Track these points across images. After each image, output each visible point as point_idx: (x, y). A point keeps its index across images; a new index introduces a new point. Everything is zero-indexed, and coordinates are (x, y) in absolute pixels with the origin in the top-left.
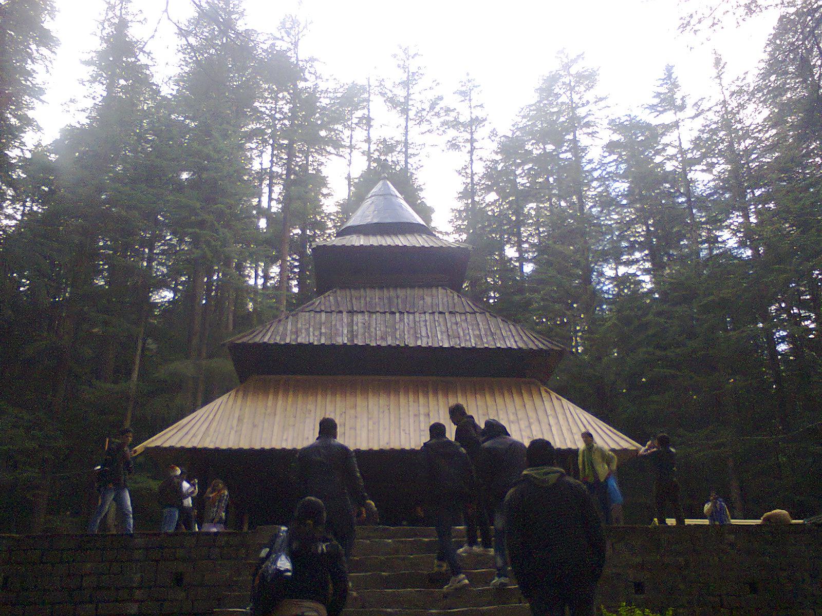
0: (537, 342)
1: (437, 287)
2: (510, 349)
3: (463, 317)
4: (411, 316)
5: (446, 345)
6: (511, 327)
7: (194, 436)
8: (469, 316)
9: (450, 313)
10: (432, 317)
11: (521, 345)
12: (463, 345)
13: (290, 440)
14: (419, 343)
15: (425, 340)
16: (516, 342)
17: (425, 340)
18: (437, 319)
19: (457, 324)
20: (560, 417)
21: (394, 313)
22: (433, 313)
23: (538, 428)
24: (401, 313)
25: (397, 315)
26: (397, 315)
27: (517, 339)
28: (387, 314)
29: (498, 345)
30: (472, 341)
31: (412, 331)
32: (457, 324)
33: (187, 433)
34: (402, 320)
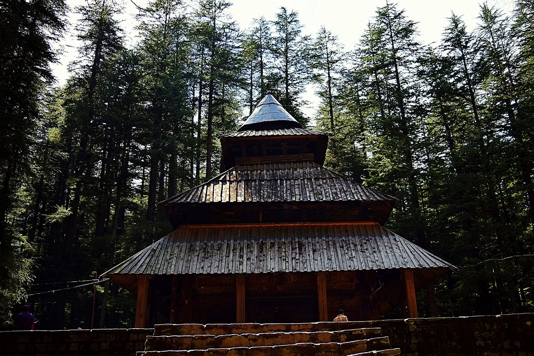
0: (376, 196)
1: (306, 162)
2: (358, 201)
5: (313, 200)
11: (364, 198)
12: (324, 199)
13: (205, 269)
14: (294, 199)
15: (298, 197)
16: (361, 196)
17: (298, 197)
18: (306, 182)
19: (320, 185)
20: (394, 247)
23: (379, 255)
27: (362, 194)
29: (349, 199)
30: (331, 196)
31: (289, 192)
32: (320, 185)
33: (136, 265)
34: (282, 184)
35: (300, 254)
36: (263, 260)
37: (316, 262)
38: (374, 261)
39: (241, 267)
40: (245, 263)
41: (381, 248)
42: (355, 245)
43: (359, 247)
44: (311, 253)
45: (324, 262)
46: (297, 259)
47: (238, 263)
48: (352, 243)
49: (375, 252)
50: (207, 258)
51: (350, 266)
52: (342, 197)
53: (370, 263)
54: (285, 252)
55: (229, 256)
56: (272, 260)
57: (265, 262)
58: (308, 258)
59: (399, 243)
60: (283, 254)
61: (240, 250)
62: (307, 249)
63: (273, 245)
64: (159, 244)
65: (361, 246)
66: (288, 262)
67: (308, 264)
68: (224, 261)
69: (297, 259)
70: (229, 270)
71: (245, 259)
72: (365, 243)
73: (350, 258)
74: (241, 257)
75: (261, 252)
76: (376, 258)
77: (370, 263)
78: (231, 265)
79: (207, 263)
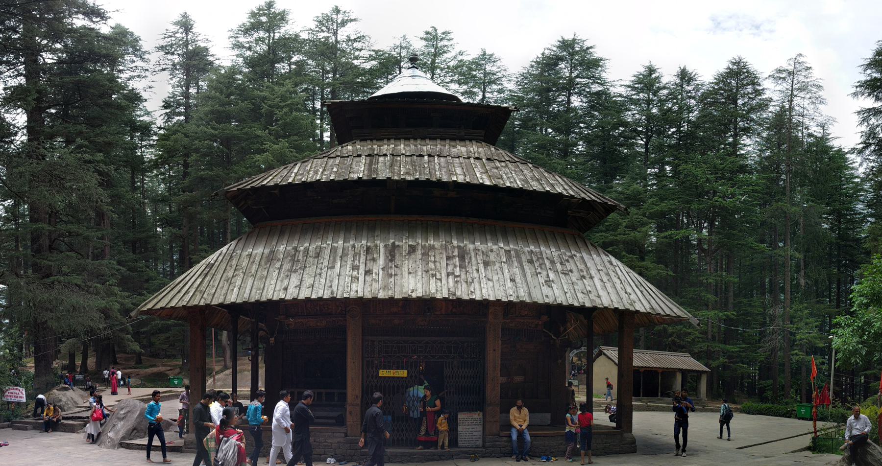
3: (503, 164)
4: (442, 159)
6: (557, 177)
8: (510, 165)
9: (488, 159)
10: (467, 161)
16: (566, 190)
20: (612, 274)
21: (422, 156)
22: (469, 158)
24: (430, 156)
25: (426, 157)
26: (426, 157)
27: (566, 187)
35: (461, 267)
36: (395, 275)
37: (490, 283)
38: (585, 291)
39: (354, 286)
41: (593, 272)
44: (481, 266)
46: (457, 276)
47: (348, 280)
49: (584, 277)
50: (296, 271)
52: (535, 186)
53: (580, 295)
54: (435, 262)
55: (333, 267)
56: (410, 276)
57: (398, 278)
58: (476, 275)
59: (617, 268)
60: (431, 265)
61: (355, 256)
62: (473, 259)
63: (412, 250)
66: (440, 280)
68: (324, 275)
69: (457, 276)
70: (332, 292)
71: (362, 271)
73: (546, 281)
74: (355, 268)
75: (391, 261)
76: (589, 288)
77: (580, 295)
79: (295, 280)
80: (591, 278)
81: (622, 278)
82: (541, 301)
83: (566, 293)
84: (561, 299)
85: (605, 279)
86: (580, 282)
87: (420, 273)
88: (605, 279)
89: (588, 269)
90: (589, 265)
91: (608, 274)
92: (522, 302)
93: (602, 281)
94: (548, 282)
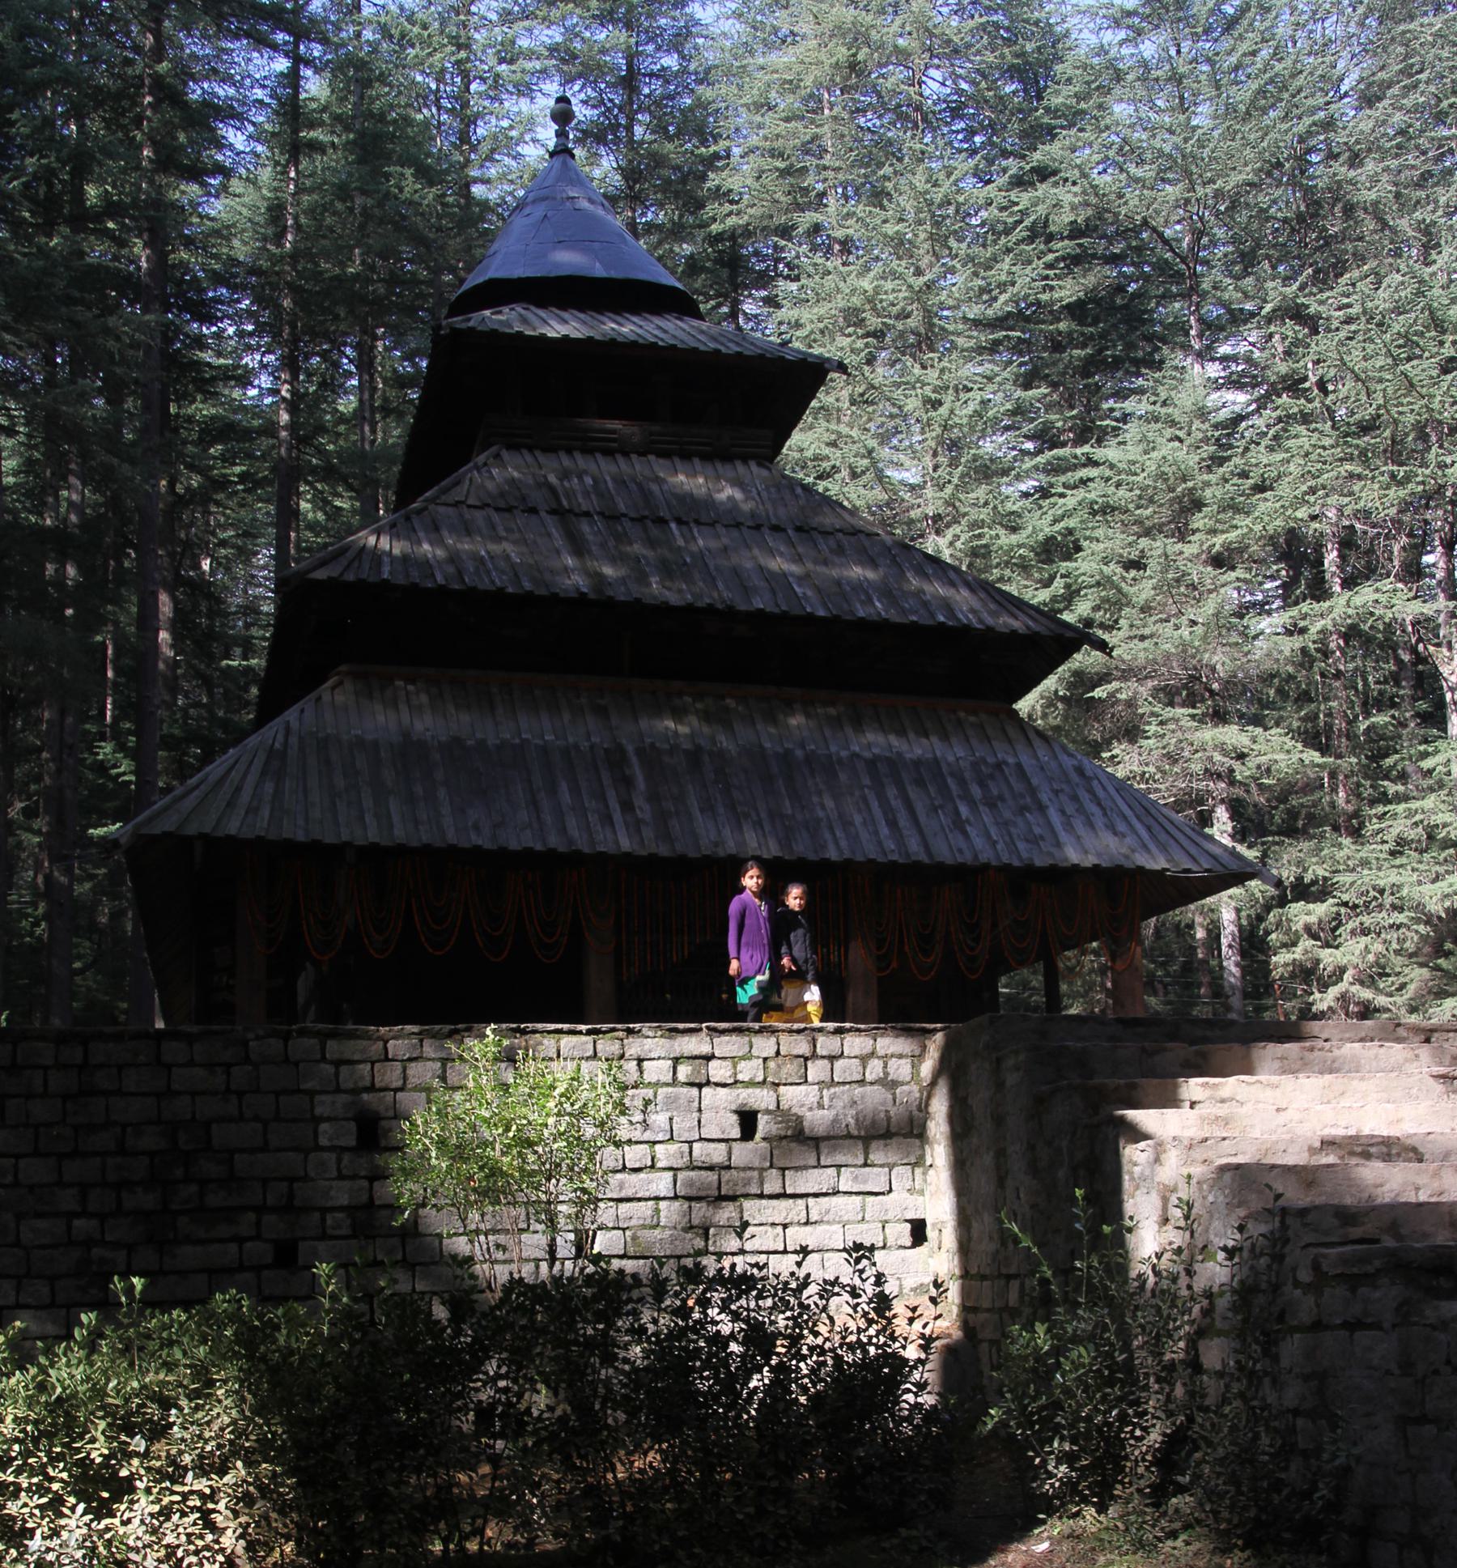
5: (821, 613)
7: (253, 810)
24: (680, 522)
28: (649, 523)
40: (617, 816)
41: (1044, 797)
42: (962, 782)
43: (976, 791)
45: (876, 833)
48: (952, 774)
51: (960, 851)
53: (1021, 846)
64: (288, 730)
65: (982, 784)
67: (827, 836)
72: (992, 777)
78: (572, 823)
80: (1042, 809)
81: (1107, 803)
82: (949, 861)
83: (995, 843)
84: (986, 856)
85: (1070, 809)
86: (1019, 820)
87: (721, 810)
88: (1070, 809)
89: (1033, 791)
90: (1035, 781)
91: (1075, 798)
92: (917, 865)
93: (1063, 812)
94: (959, 825)
